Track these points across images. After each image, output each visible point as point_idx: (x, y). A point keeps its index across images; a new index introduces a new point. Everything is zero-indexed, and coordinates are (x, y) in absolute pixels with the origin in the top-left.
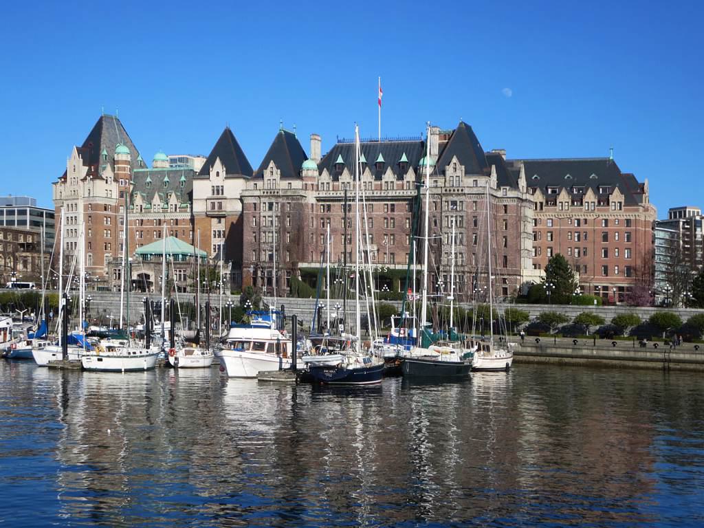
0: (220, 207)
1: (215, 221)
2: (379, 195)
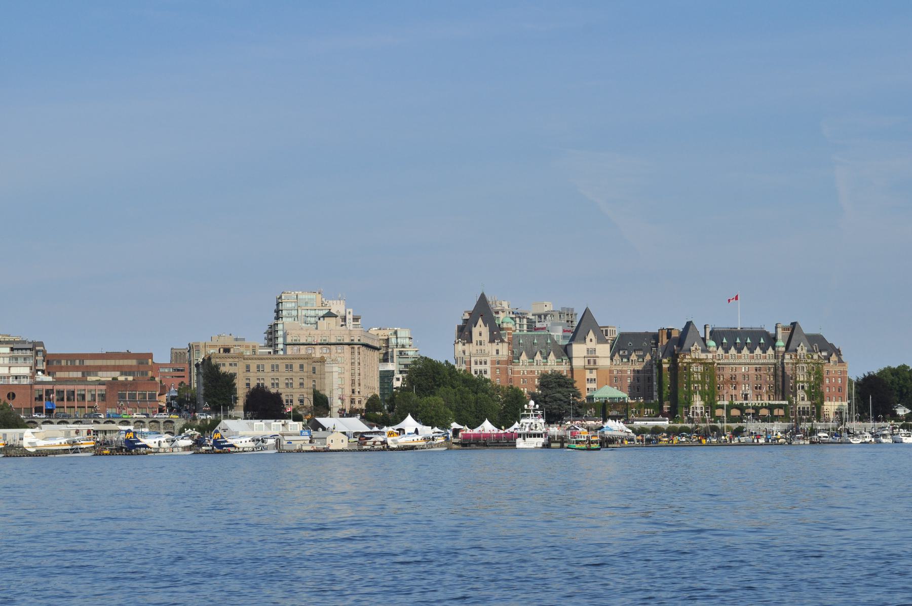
0: (595, 362)
1: (588, 371)
2: (754, 362)
